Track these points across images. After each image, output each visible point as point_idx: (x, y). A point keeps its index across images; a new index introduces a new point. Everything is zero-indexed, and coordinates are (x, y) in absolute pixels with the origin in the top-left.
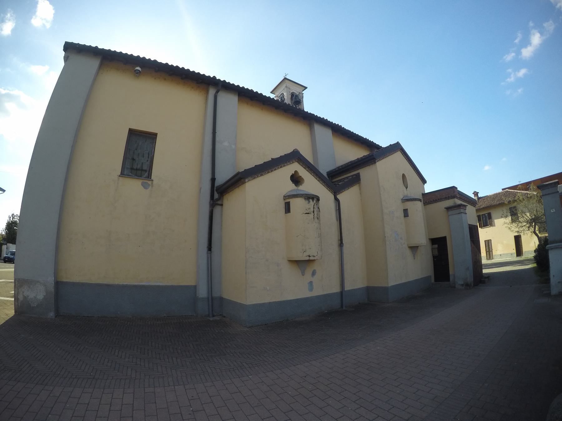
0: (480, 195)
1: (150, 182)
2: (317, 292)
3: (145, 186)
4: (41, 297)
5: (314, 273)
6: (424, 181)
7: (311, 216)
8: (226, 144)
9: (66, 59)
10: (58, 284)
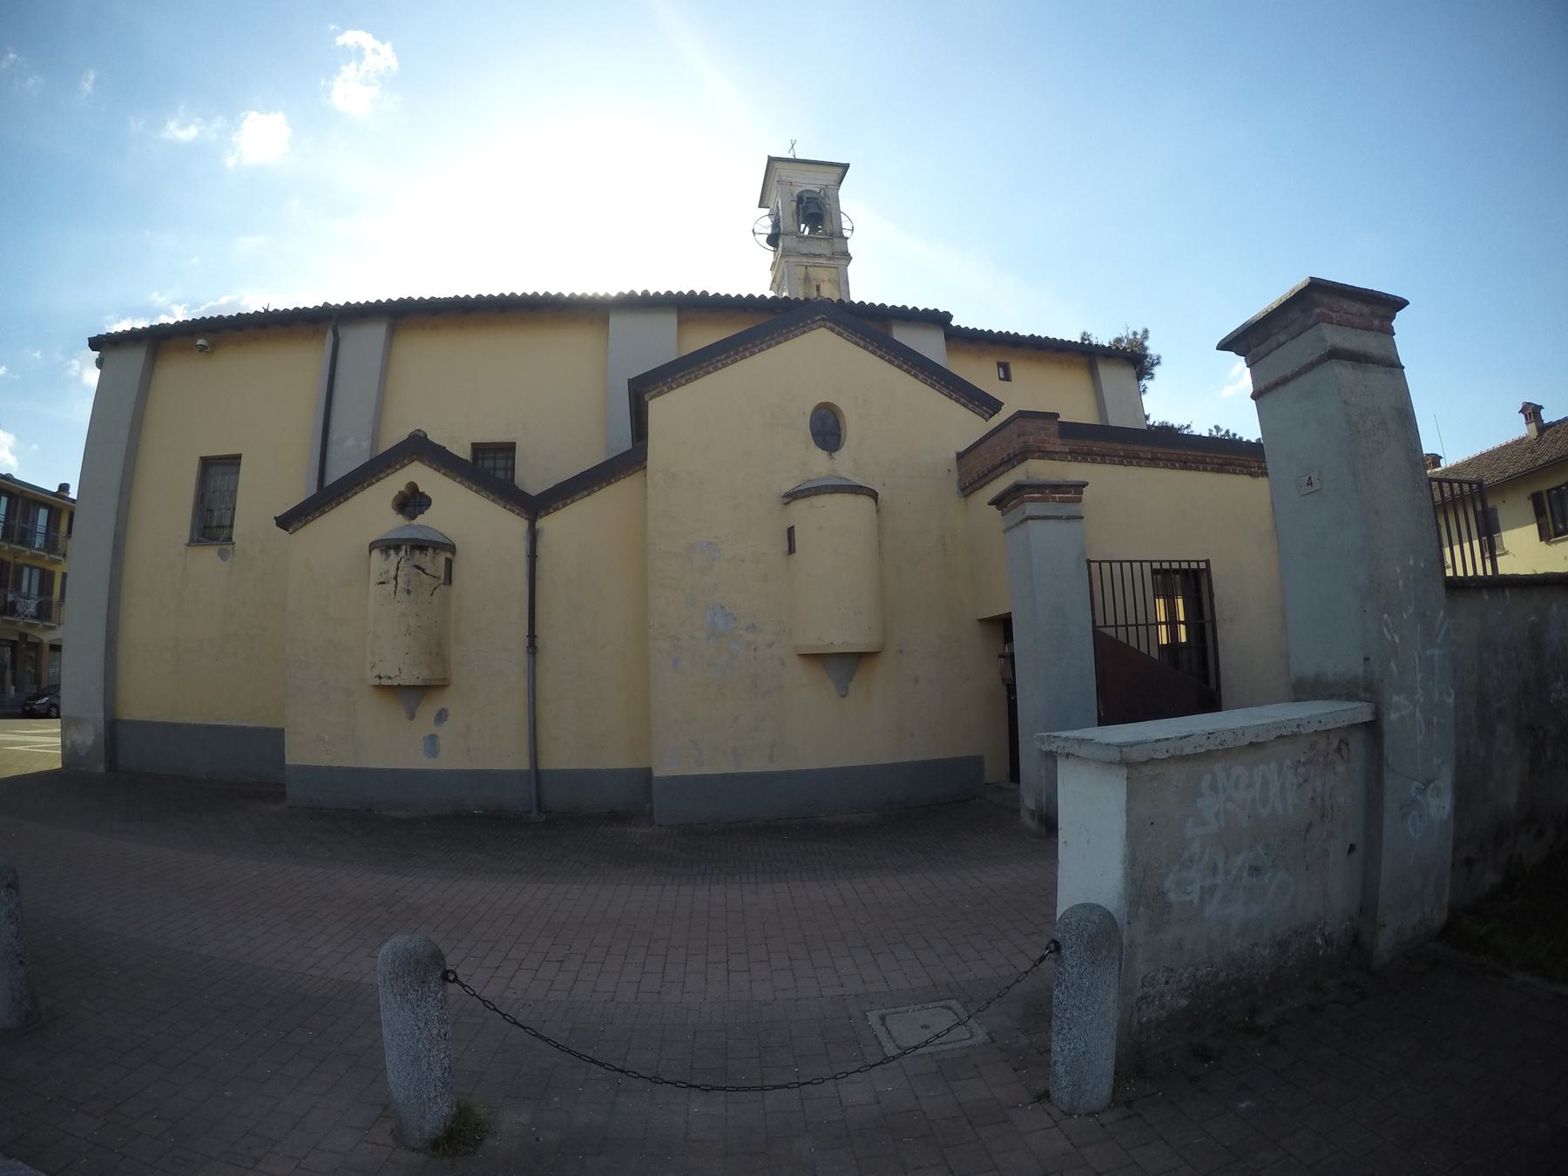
0: (1548, 417)
1: (229, 548)
2: (450, 759)
3: (223, 555)
4: (89, 741)
5: (441, 716)
6: (1057, 415)
7: (390, 587)
8: (350, 443)
9: (100, 363)
10: (113, 726)
